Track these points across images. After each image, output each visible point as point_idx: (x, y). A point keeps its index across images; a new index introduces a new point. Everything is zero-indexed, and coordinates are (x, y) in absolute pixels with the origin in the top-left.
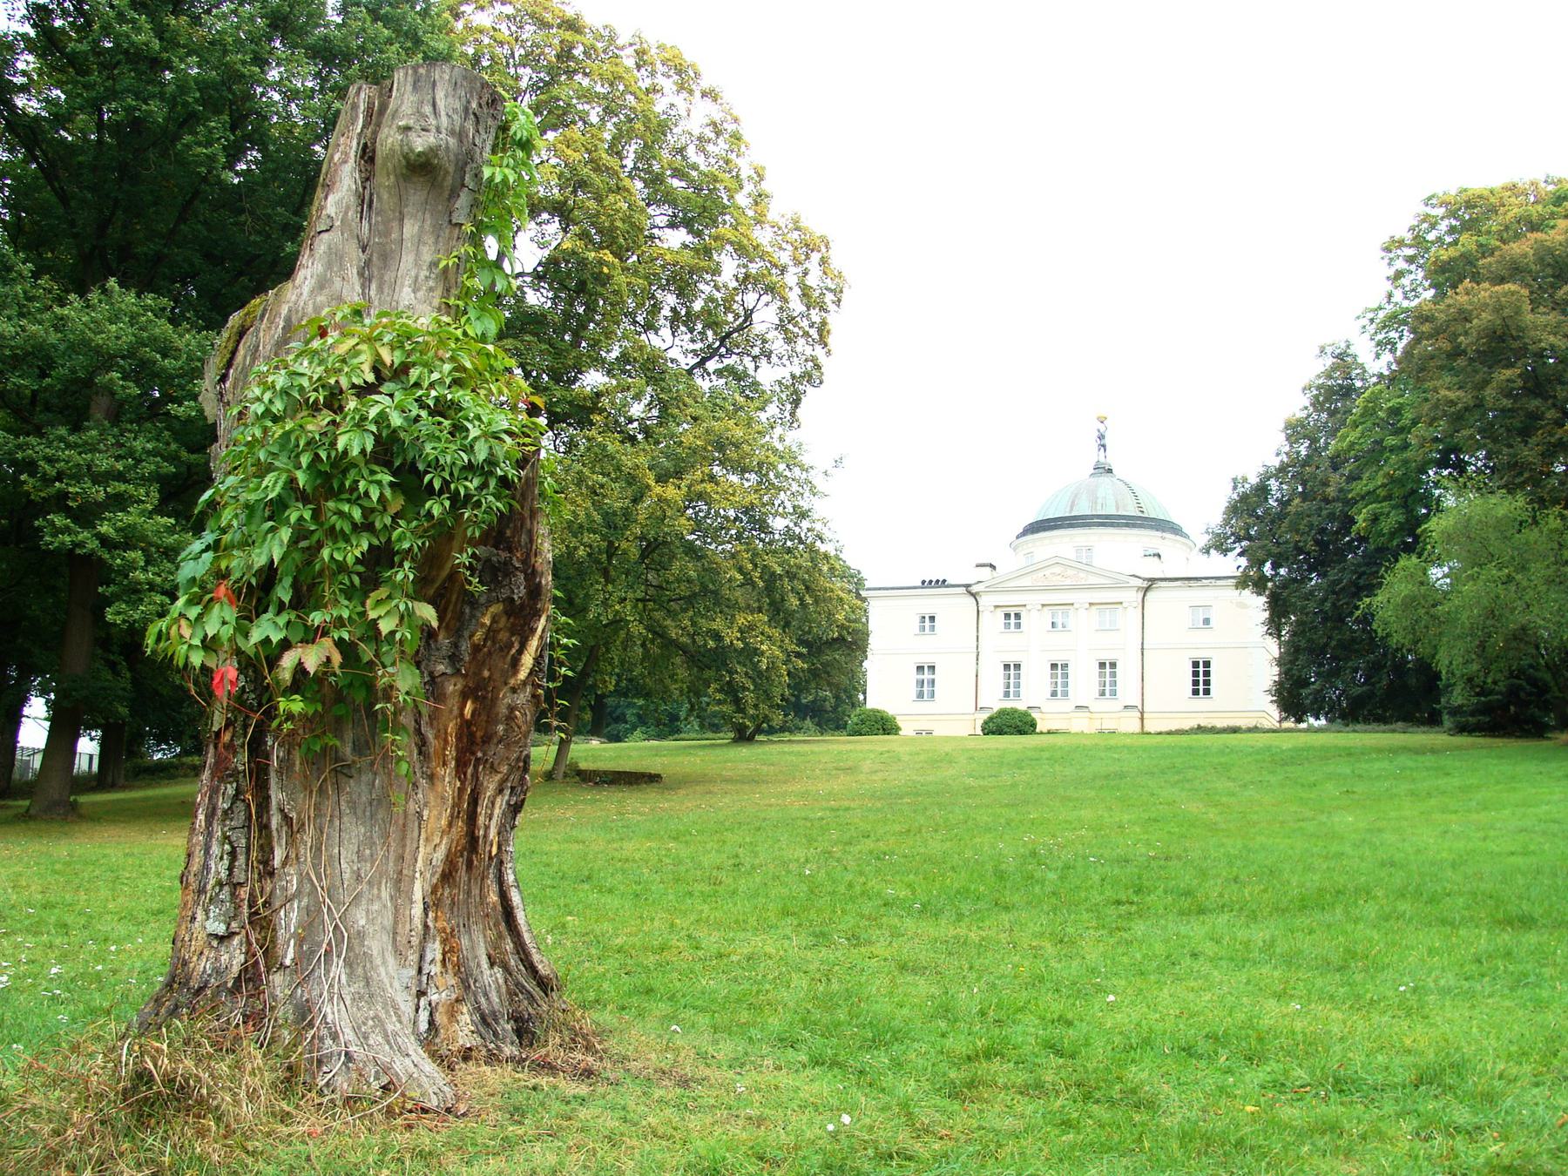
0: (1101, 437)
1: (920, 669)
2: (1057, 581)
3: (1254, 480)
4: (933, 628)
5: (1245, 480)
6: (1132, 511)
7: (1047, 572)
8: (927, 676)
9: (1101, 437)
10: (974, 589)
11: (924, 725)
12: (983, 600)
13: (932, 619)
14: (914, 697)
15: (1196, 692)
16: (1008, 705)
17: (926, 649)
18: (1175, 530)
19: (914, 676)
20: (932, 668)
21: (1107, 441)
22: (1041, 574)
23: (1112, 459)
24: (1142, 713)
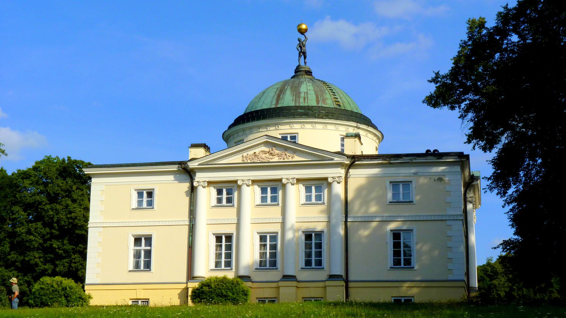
0: (301, 45)
1: (138, 241)
2: (265, 157)
3: (491, 23)
4: (150, 204)
5: (482, 25)
6: (330, 103)
7: (257, 150)
8: (143, 247)
9: (301, 45)
10: (192, 165)
11: (142, 294)
12: (200, 177)
13: (150, 194)
14: (131, 267)
15: (397, 263)
16: (220, 274)
17: (144, 223)
18: (367, 122)
19: (132, 247)
20: (149, 240)
21: (308, 49)
22: (251, 152)
23: (311, 64)
24: (347, 281)
